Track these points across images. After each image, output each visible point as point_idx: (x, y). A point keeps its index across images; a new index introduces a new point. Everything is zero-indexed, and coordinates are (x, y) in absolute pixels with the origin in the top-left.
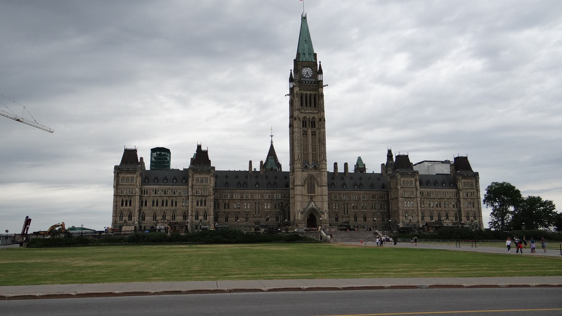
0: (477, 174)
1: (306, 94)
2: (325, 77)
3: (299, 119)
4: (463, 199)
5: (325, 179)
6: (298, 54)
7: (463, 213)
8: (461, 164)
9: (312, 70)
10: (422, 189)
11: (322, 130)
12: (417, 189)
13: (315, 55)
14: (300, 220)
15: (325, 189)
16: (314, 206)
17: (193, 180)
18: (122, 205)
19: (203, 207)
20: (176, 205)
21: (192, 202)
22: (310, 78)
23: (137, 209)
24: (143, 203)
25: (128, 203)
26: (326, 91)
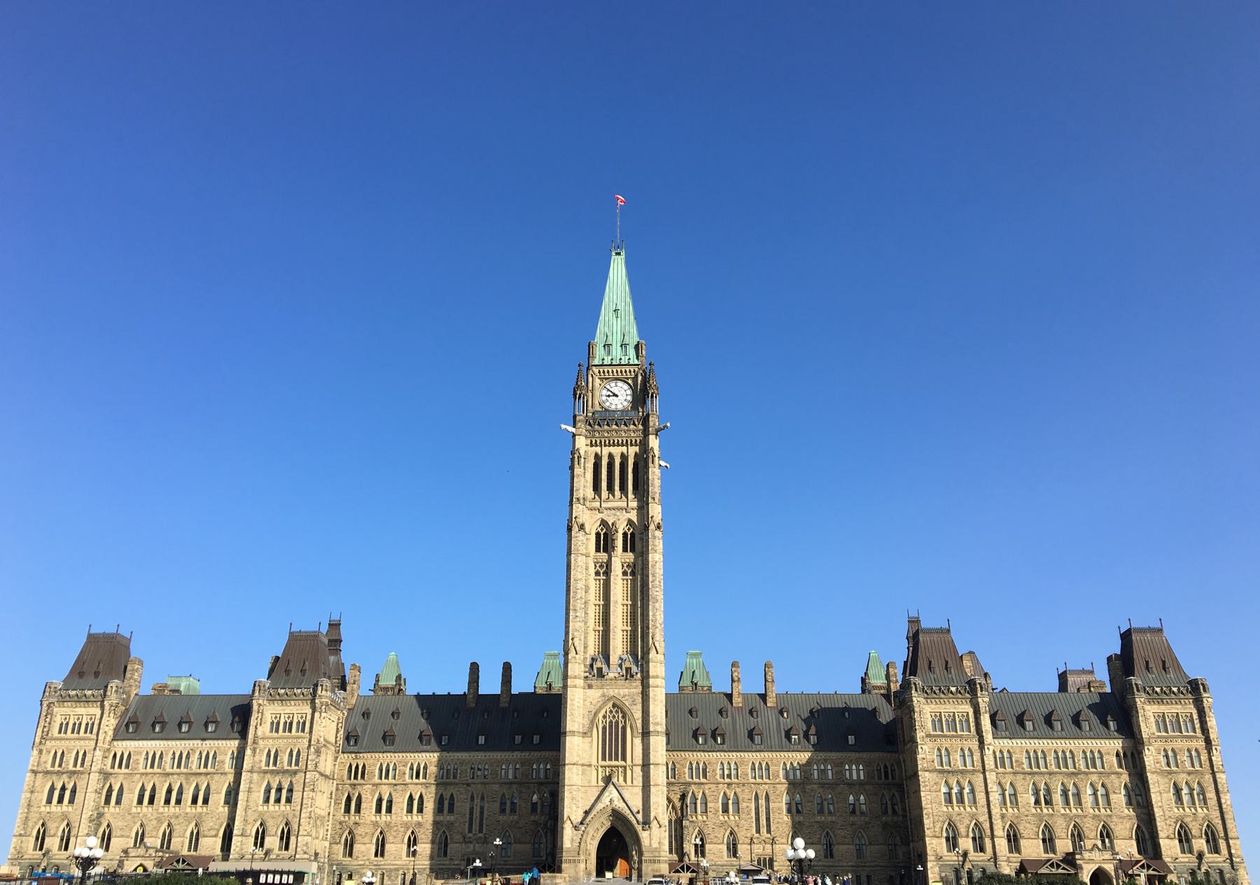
1: (611, 456)
4: (1161, 773)
7: (1160, 824)
10: (1006, 744)
14: (569, 850)
15: (658, 744)
16: (619, 805)
18: (49, 801)
19: (283, 805)
20: (206, 801)
21: (249, 791)
23: (87, 814)
24: (110, 796)
25: (68, 793)
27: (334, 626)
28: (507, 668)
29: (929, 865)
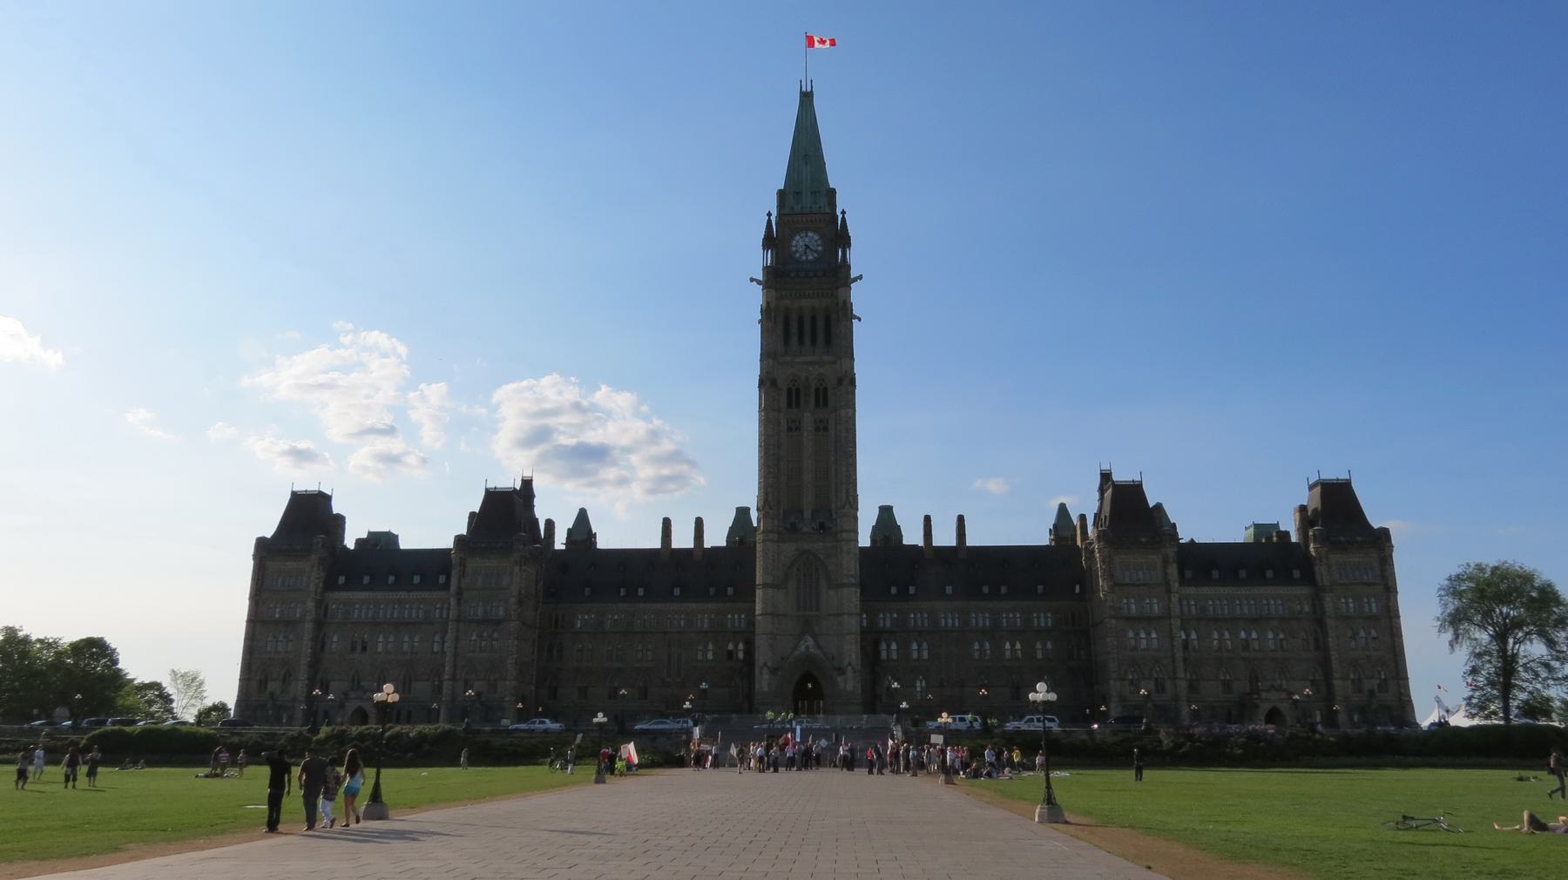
0: (1384, 534)
2: (858, 258)
3: (774, 383)
5: (851, 566)
6: (781, 194)
7: (1335, 665)
8: (1336, 506)
9: (822, 238)
10: (1191, 590)
11: (843, 412)
12: (1169, 591)
13: (833, 192)
17: (463, 574)
21: (457, 639)
22: (816, 260)
23: (305, 660)
26: (858, 296)
27: (527, 484)
28: (699, 523)
29: (1113, 705)
